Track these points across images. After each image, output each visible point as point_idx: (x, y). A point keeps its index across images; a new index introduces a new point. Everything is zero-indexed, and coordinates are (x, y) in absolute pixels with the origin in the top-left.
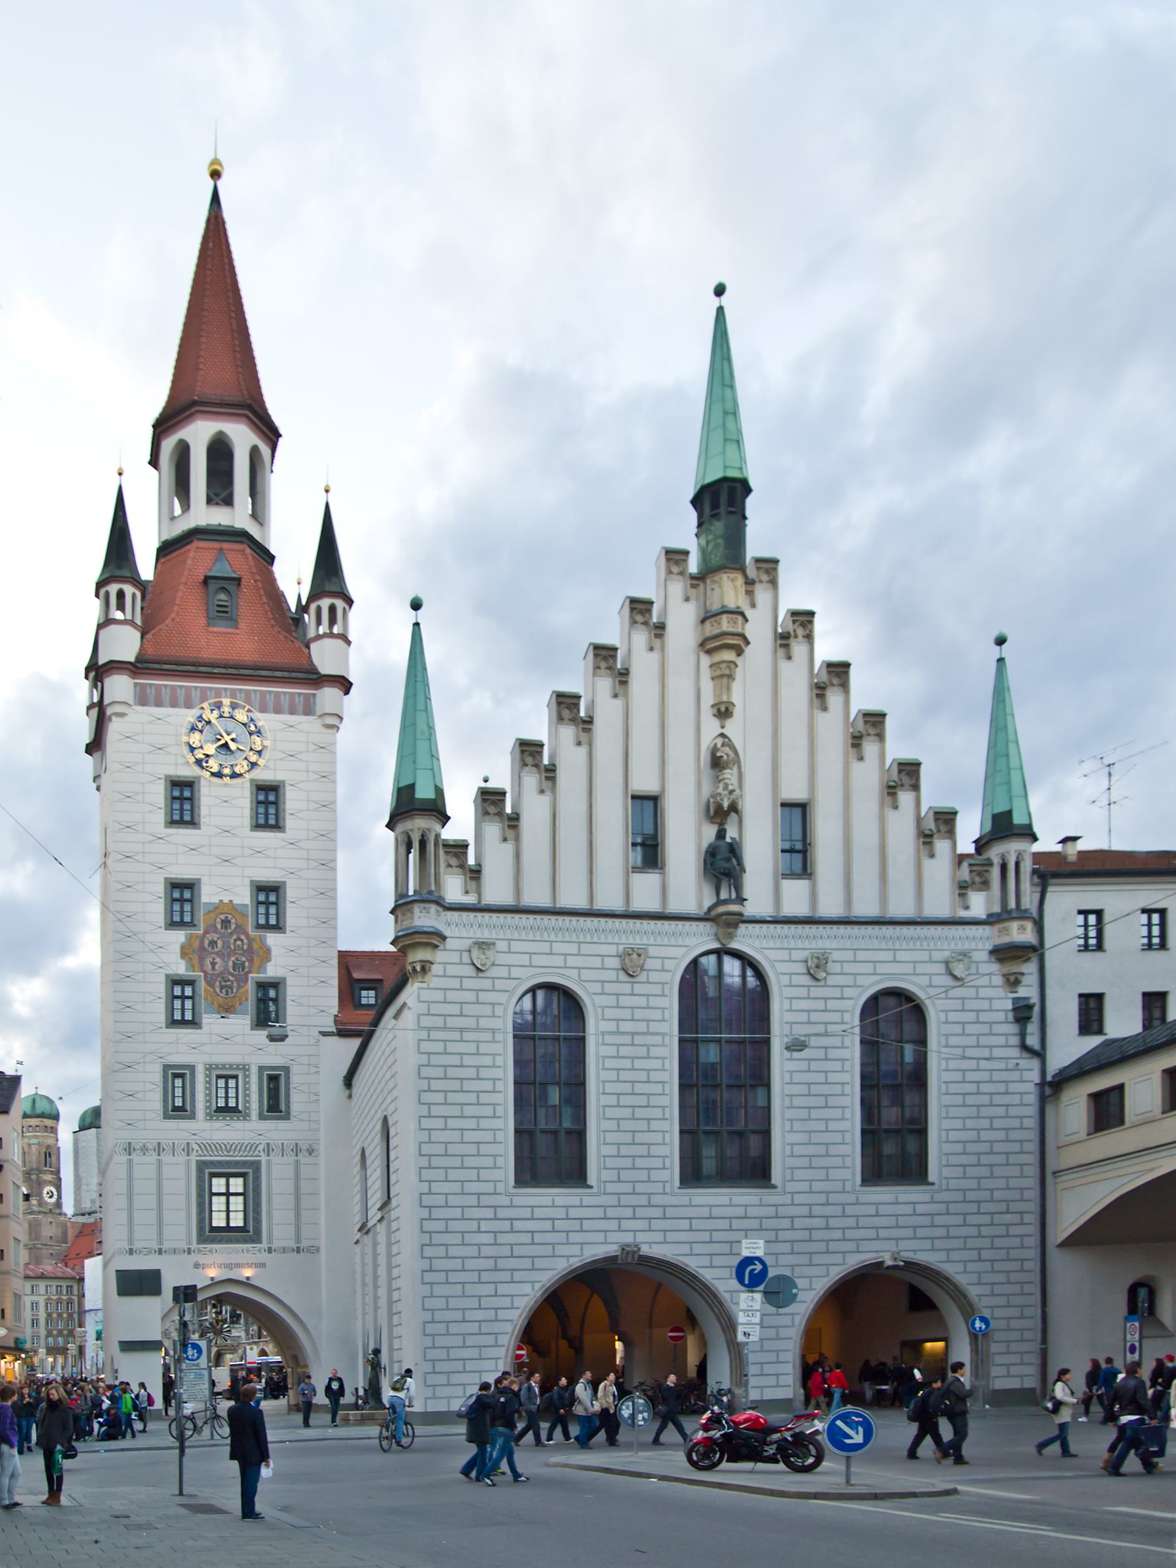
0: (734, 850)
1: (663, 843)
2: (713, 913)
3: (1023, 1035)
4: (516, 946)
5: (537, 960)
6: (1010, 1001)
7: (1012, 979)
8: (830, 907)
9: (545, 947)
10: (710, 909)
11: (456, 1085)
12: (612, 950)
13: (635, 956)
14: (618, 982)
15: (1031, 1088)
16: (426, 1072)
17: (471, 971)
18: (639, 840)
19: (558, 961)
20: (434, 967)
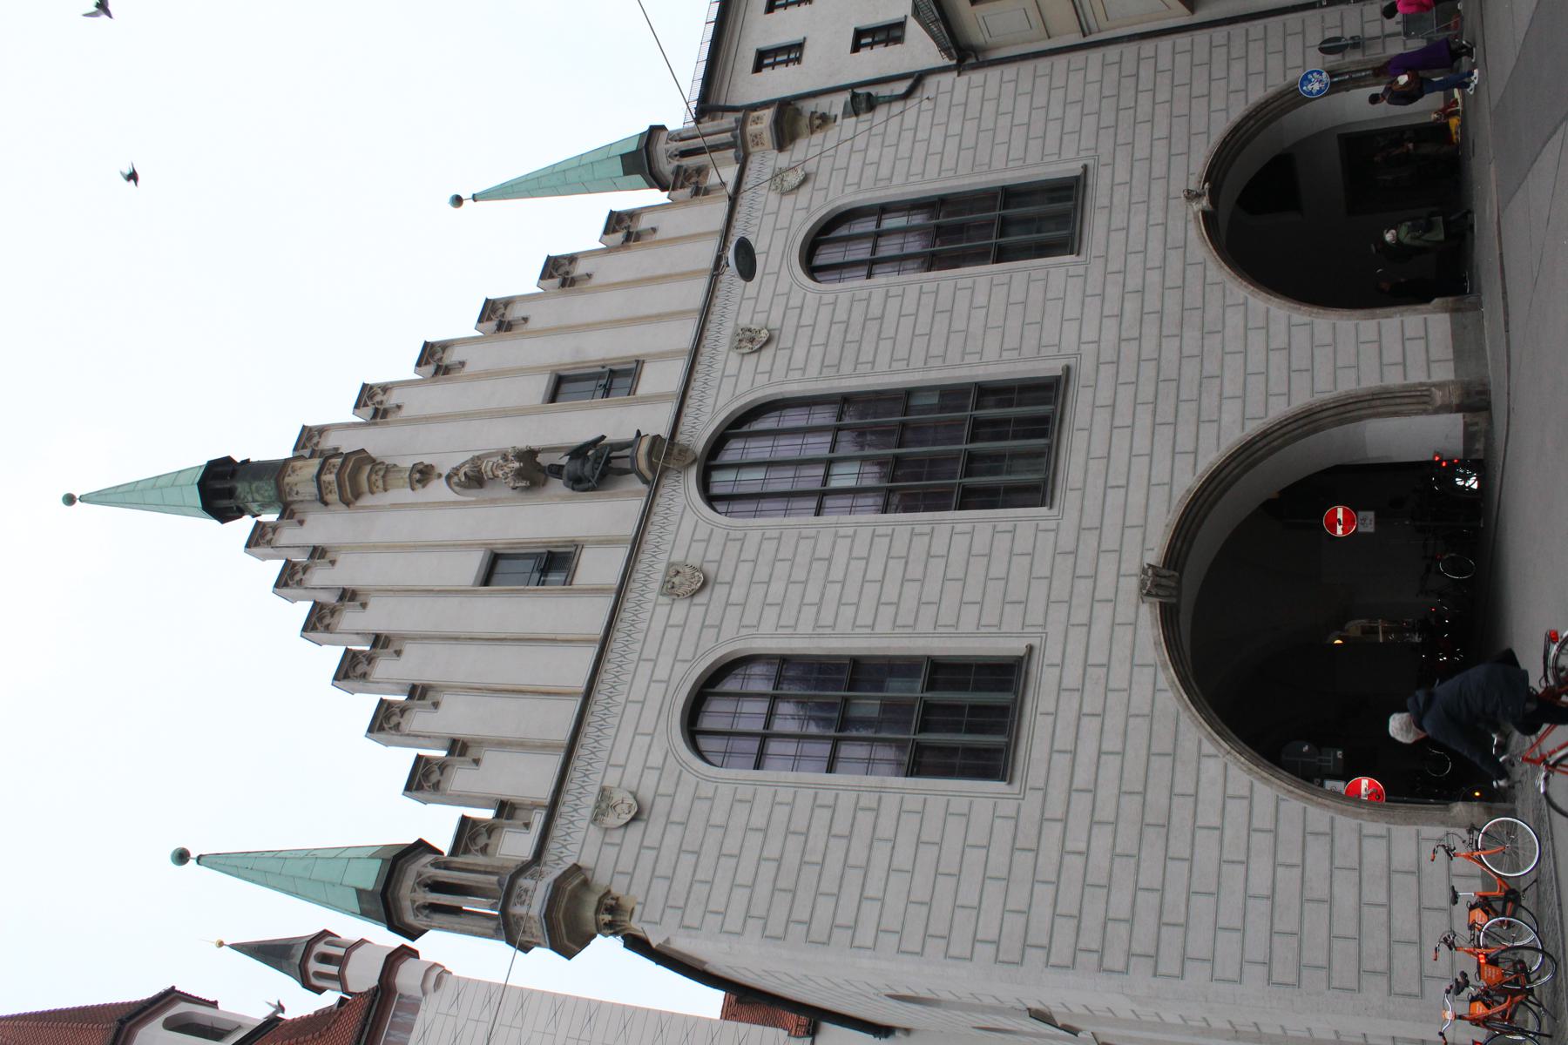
0: (578, 453)
1: (547, 544)
2: (649, 476)
3: (892, 99)
4: (619, 758)
5: (646, 726)
6: (846, 121)
7: (817, 122)
8: (683, 334)
9: (633, 710)
10: (645, 481)
11: (810, 874)
12: (662, 611)
13: (676, 580)
14: (708, 605)
15: (964, 78)
16: (776, 927)
17: (637, 828)
18: (536, 576)
19: (657, 691)
20: (615, 891)
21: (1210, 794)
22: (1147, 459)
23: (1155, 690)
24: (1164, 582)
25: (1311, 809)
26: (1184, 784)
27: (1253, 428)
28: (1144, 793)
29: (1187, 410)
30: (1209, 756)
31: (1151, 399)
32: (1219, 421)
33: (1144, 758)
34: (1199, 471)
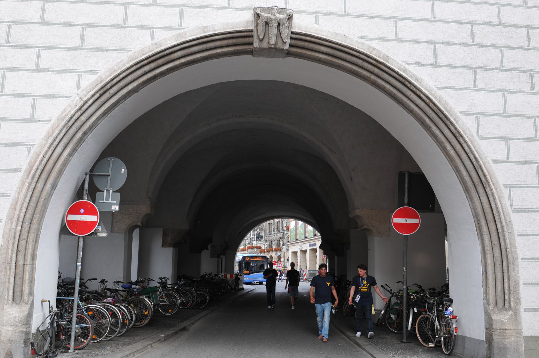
21: (37, 83)
22: (429, 16)
23: (153, 29)
24: (273, 31)
25: (19, 176)
26: (49, 59)
27: (465, 125)
28: (42, 22)
29: (491, 57)
30: (79, 81)
31: (504, 20)
32: (475, 88)
33: (80, 21)
34: (411, 68)
